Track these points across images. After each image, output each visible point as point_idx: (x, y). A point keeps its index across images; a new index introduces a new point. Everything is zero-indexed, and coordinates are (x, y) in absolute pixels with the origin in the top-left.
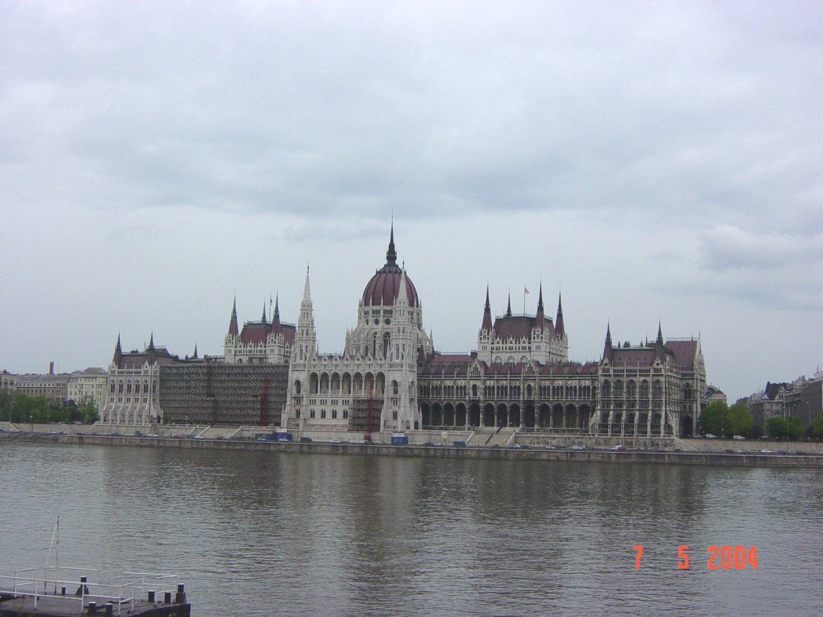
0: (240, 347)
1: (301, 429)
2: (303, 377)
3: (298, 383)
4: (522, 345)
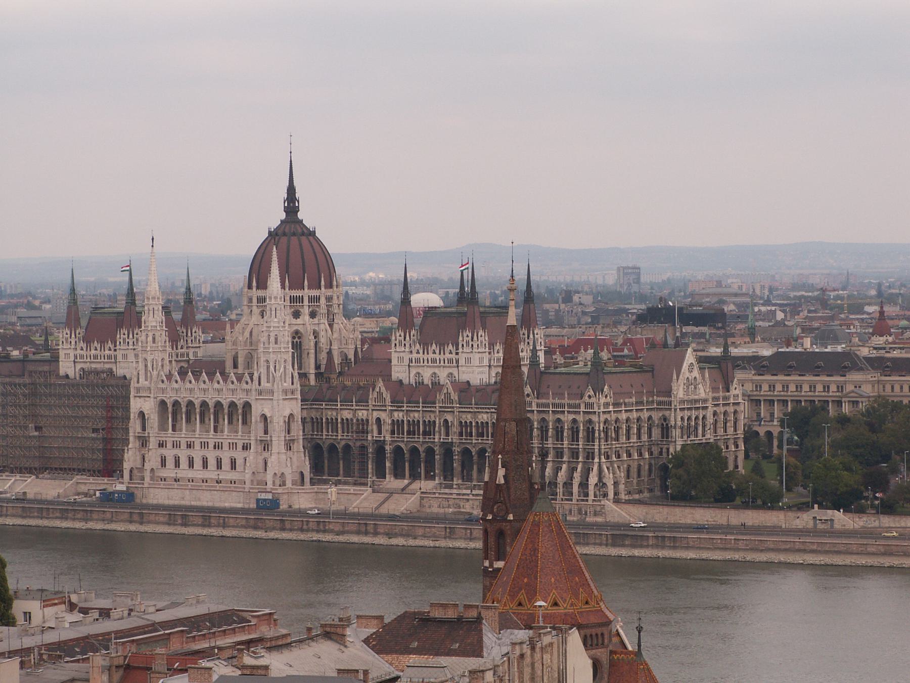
0: (82, 349)
1: (146, 485)
2: (149, 406)
3: (142, 415)
4: (448, 355)
